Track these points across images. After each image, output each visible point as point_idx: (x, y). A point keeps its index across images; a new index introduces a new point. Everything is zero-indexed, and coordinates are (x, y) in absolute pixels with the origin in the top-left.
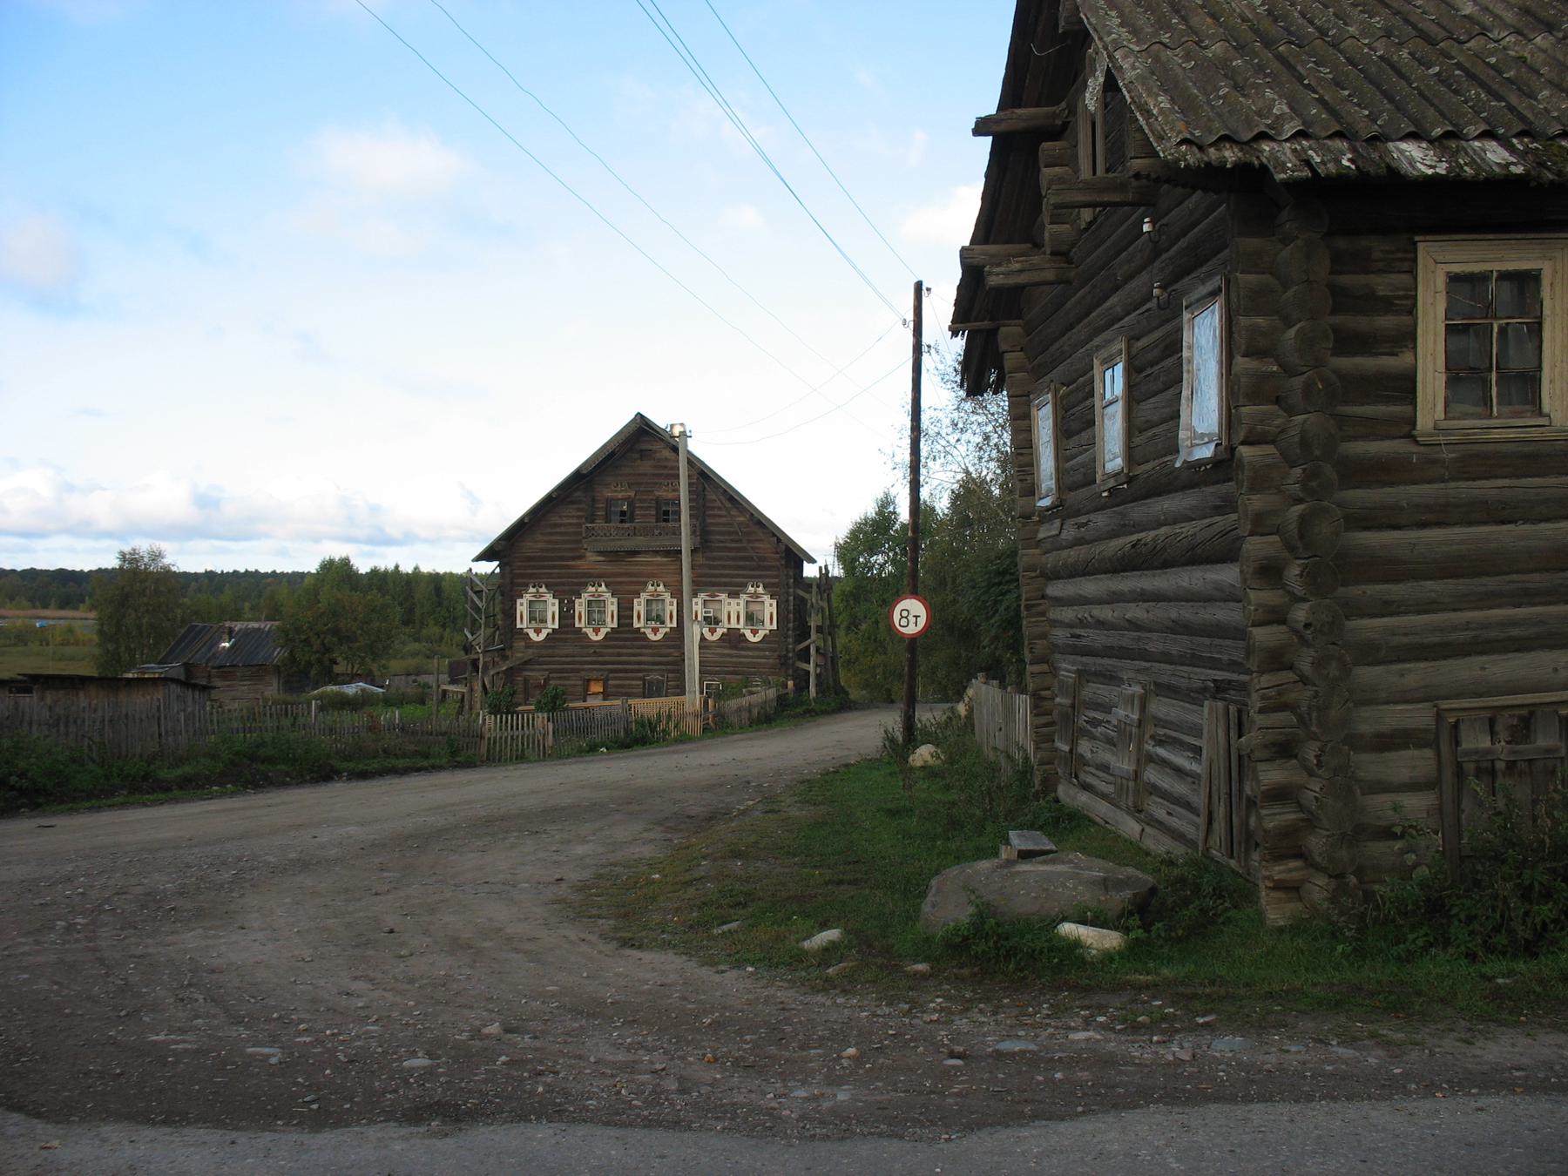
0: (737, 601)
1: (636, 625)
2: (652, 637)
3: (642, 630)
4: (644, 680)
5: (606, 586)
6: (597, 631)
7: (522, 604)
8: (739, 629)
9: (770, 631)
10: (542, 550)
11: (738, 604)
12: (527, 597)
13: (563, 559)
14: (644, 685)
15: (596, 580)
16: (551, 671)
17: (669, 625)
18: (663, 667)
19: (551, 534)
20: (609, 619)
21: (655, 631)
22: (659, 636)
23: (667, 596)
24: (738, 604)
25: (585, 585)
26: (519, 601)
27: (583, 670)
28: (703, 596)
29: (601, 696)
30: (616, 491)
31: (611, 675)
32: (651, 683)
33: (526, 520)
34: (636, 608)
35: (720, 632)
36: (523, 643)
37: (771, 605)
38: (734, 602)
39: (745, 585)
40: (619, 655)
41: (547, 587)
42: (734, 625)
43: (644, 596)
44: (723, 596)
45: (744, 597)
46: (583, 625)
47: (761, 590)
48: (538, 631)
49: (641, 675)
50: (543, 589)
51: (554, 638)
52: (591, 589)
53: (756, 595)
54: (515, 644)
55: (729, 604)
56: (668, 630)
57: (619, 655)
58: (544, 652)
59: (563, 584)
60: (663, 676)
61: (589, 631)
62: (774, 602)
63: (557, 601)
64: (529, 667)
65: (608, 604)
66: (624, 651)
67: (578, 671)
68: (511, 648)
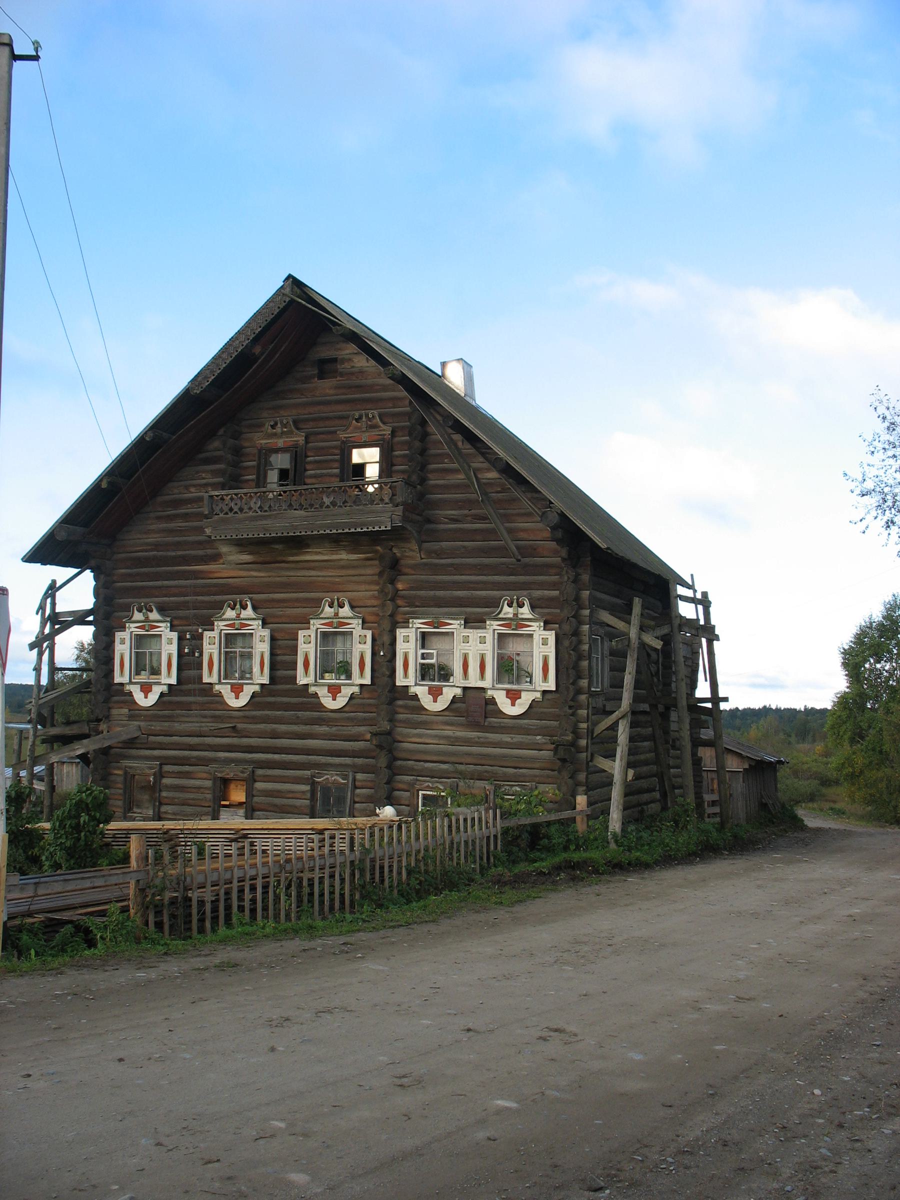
0: (480, 633)
1: (302, 680)
2: (329, 703)
3: (312, 689)
4: (313, 784)
5: (254, 608)
6: (237, 690)
7: (123, 642)
8: (483, 689)
9: (544, 692)
10: (157, 546)
11: (483, 641)
12: (133, 628)
13: (186, 561)
14: (313, 792)
15: (238, 598)
16: (165, 761)
17: (357, 680)
18: (348, 761)
19: (170, 518)
20: (256, 669)
21: (334, 691)
22: (341, 702)
23: (355, 625)
24: (483, 641)
25: (219, 606)
26: (119, 635)
27: (215, 760)
28: (418, 624)
29: (241, 812)
30: (275, 435)
31: (260, 772)
32: (326, 790)
33: (104, 485)
34: (302, 648)
35: (449, 693)
36: (125, 711)
37: (545, 642)
38: (474, 634)
39: (495, 604)
40: (275, 735)
41: (162, 610)
42: (474, 681)
43: (316, 624)
44: (455, 625)
45: (494, 626)
46: (214, 679)
47: (525, 612)
48: (146, 689)
49: (308, 773)
50: (154, 615)
51: (170, 702)
52: (230, 614)
53: (517, 622)
54: (114, 712)
55: (466, 640)
56: (356, 689)
57: (275, 735)
58: (157, 726)
59: (184, 606)
60: (345, 777)
61: (225, 690)
62: (551, 636)
63: (174, 635)
64: (134, 752)
65: (256, 639)
66: (283, 728)
67: (205, 762)
68: (108, 717)
